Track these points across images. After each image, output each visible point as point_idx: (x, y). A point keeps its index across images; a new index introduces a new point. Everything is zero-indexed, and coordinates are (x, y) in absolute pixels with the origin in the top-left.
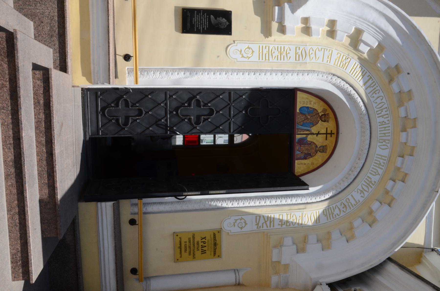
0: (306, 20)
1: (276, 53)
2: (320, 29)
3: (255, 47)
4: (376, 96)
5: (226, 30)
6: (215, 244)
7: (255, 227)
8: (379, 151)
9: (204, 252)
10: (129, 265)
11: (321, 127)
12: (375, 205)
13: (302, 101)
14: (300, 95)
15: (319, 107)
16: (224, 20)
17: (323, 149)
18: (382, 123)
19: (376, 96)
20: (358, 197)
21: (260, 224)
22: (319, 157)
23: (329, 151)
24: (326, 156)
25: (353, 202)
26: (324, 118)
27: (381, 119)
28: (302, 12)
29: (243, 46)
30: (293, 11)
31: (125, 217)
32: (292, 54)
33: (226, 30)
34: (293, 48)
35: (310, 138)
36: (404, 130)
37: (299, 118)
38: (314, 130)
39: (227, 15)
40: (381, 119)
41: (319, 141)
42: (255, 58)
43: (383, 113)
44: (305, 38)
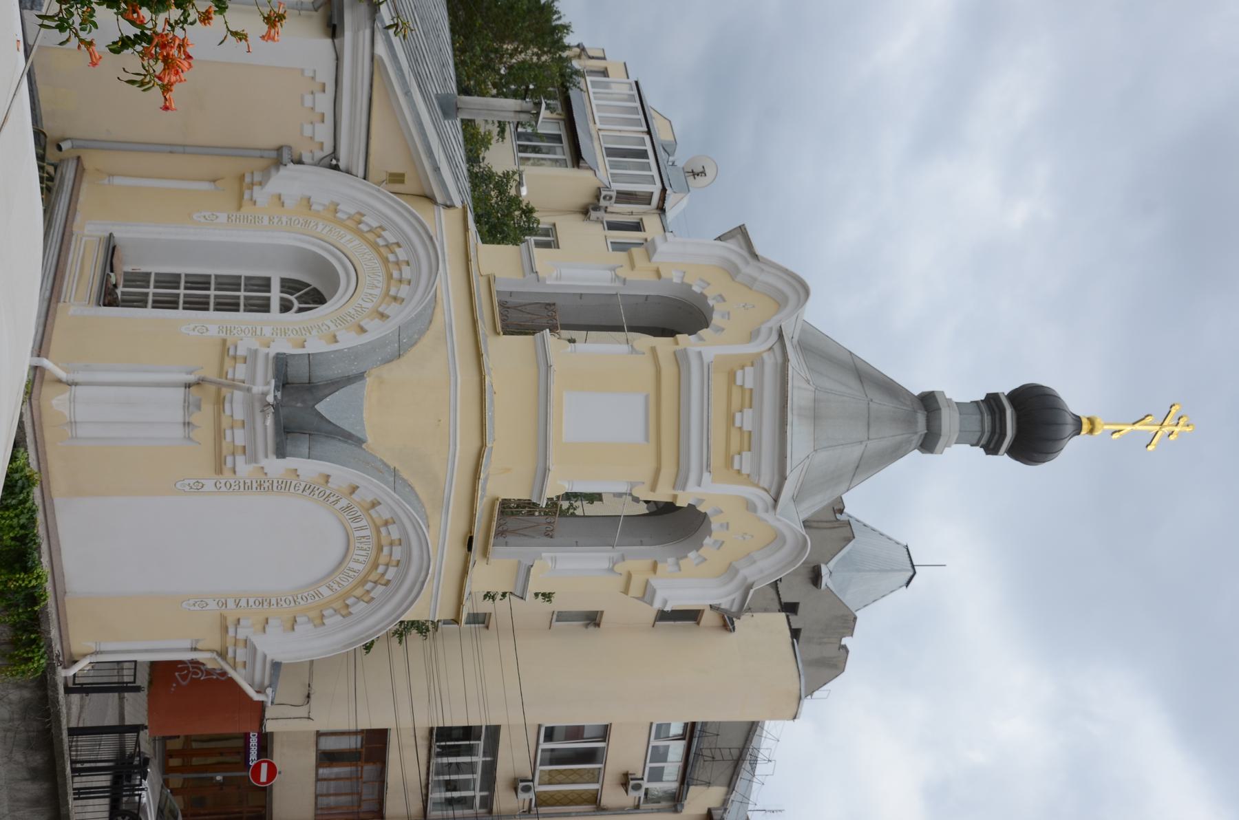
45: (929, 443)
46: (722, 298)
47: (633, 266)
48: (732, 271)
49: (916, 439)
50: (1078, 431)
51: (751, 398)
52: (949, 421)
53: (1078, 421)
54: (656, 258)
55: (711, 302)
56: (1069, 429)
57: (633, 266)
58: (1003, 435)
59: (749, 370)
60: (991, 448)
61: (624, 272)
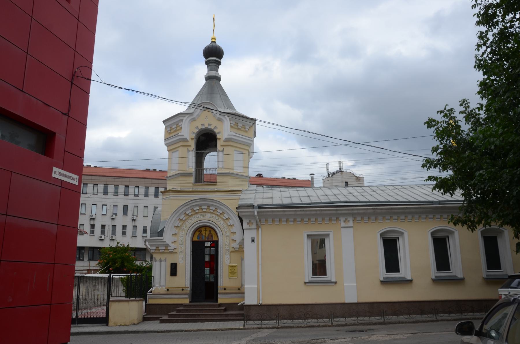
2: (175, 238)
3: (180, 256)
10: (238, 291)
11: (203, 232)
13: (196, 239)
14: (194, 240)
15: (197, 233)
17: (210, 231)
20: (222, 223)
22: (213, 232)
23: (211, 229)
24: (212, 230)
26: (200, 231)
28: (170, 244)
31: (224, 291)
32: (181, 246)
35: (207, 236)
37: (201, 240)
38: (204, 235)
39: (172, 264)
41: (207, 233)
42: (182, 256)
45: (218, 79)
46: (203, 125)
47: (190, 146)
48: (194, 120)
49: (217, 81)
50: (215, 42)
51: (237, 124)
52: (213, 73)
53: (212, 42)
54: (188, 139)
55: (203, 127)
56: (214, 44)
57: (190, 146)
58: (215, 60)
59: (231, 122)
60: (219, 63)
61: (191, 149)
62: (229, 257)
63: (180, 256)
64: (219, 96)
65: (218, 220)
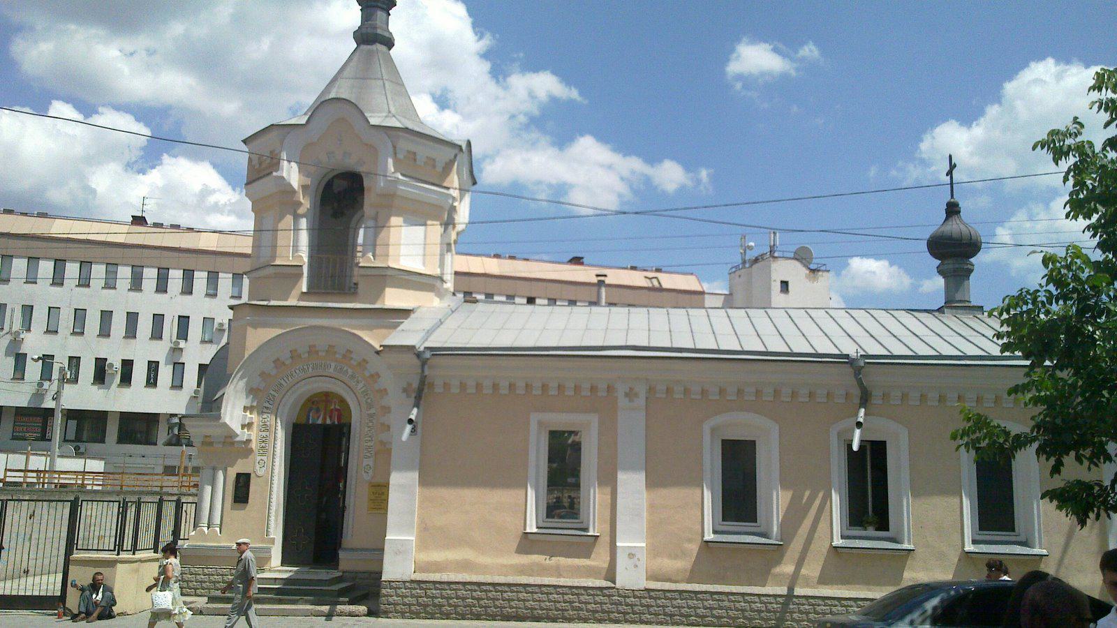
0: (243, 427)
1: (263, 444)
3: (259, 458)
4: (294, 374)
5: (248, 476)
6: (379, 486)
7: (371, 459)
8: (332, 370)
9: (383, 493)
12: (367, 374)
16: (242, 478)
18: (313, 368)
19: (294, 374)
20: (361, 385)
21: (370, 455)
25: (365, 388)
27: (310, 370)
28: (238, 430)
29: (258, 467)
30: (237, 435)
33: (248, 476)
34: (260, 433)
36: (317, 352)
39: (239, 475)
40: (310, 370)
43: (305, 367)
44: (255, 426)
62: (370, 462)
63: (259, 458)
64: (380, 83)
65: (353, 377)
